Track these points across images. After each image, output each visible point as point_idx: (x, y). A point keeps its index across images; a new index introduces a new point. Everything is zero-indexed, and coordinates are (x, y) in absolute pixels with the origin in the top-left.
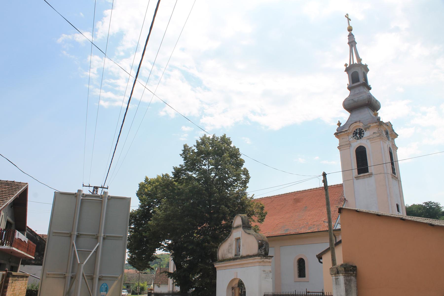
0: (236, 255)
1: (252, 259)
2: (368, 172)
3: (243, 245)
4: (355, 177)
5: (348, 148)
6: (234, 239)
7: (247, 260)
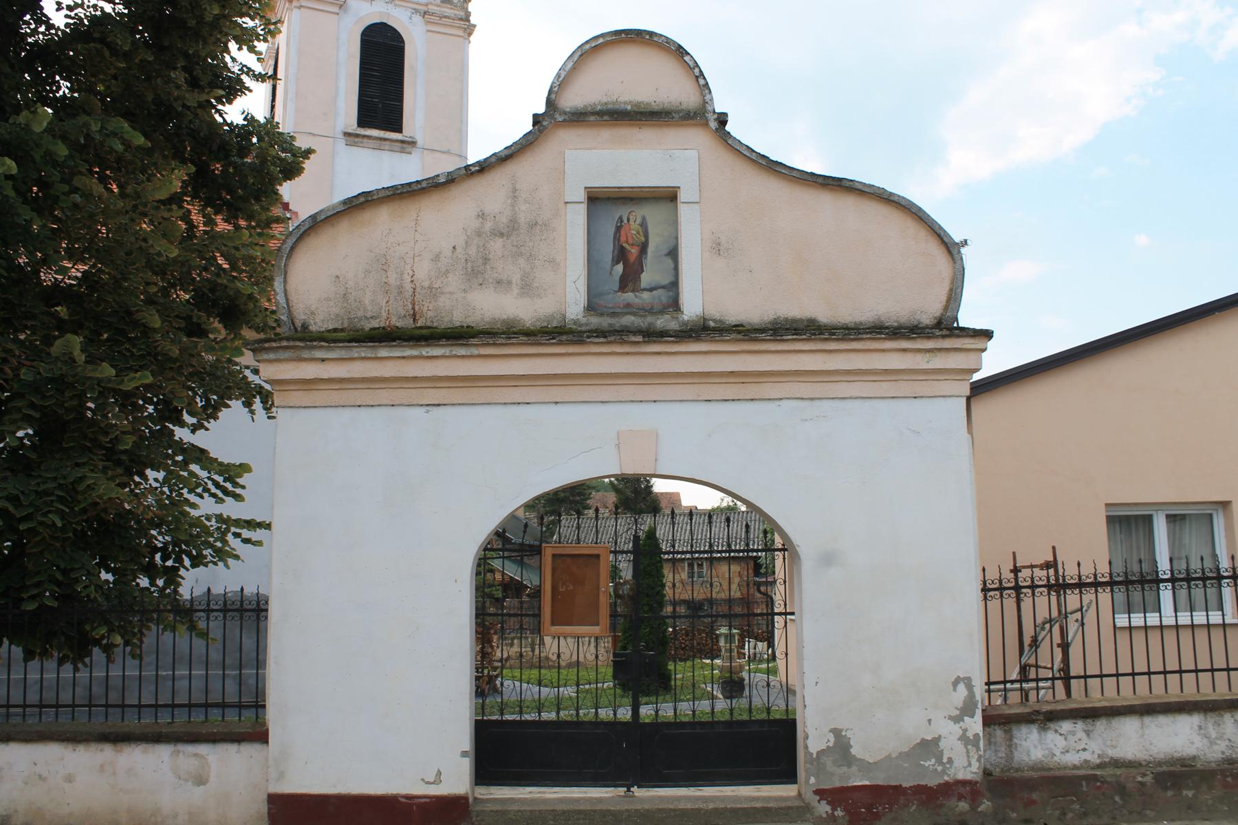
0: (591, 308)
1: (904, 350)
2: (399, 129)
3: (717, 248)
4: (347, 134)
5: (336, 9)
6: (581, 196)
7: (904, 350)
